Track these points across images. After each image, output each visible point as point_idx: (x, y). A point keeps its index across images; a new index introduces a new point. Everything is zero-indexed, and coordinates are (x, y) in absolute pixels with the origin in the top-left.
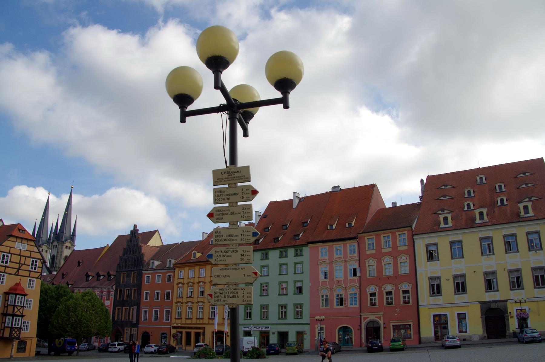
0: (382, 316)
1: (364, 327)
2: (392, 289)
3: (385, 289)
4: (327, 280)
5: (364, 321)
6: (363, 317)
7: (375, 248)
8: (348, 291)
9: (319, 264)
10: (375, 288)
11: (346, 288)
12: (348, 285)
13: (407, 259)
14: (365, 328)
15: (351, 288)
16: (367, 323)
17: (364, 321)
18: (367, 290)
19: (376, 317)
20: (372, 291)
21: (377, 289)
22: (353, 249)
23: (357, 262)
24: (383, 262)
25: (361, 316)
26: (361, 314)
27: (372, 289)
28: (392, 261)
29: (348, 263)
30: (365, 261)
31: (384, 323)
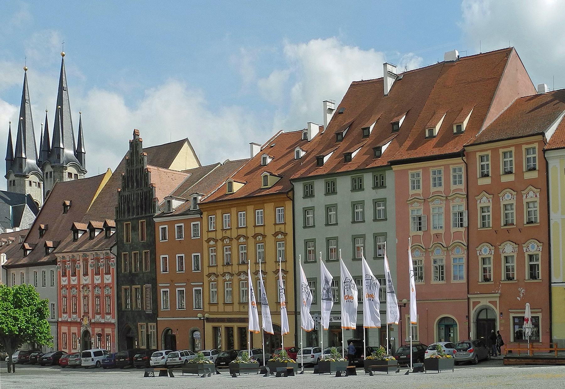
0: (497, 300)
1: (473, 318)
2: (514, 251)
3: (504, 252)
6: (471, 301)
13: (536, 196)
14: (475, 321)
15: (455, 249)
16: (477, 312)
19: (490, 302)
24: (501, 200)
25: (468, 299)
26: (469, 296)
28: (515, 199)
29: (451, 201)
31: (501, 314)
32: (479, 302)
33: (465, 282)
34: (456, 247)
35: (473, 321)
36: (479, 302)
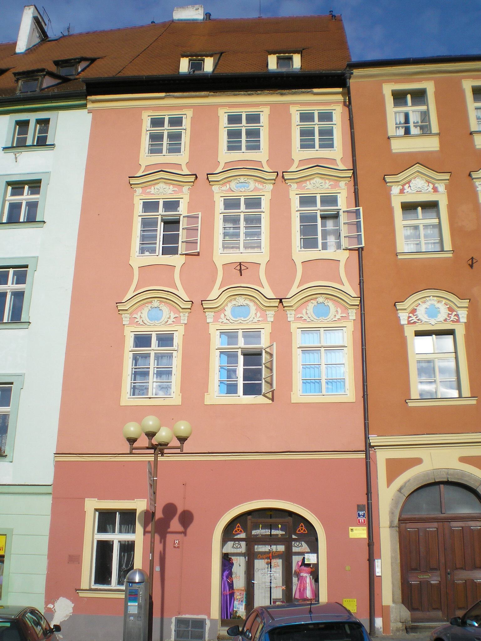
1: (392, 513)
4: (177, 260)
5: (390, 481)
7: (435, 129)
8: (291, 318)
9: (133, 181)
10: (451, 309)
11: (281, 301)
12: (294, 290)
17: (390, 481)
18: (403, 317)
20: (433, 321)
21: (463, 315)
22: (321, 133)
23: (342, 184)
27: (432, 312)
29: (294, 186)
30: (388, 179)
32: (418, 461)
33: (353, 400)
34: (314, 302)
35: (391, 522)
36: (418, 461)
